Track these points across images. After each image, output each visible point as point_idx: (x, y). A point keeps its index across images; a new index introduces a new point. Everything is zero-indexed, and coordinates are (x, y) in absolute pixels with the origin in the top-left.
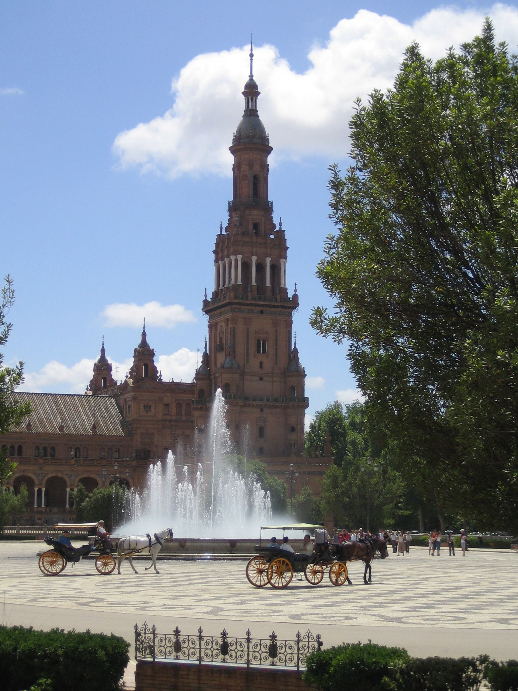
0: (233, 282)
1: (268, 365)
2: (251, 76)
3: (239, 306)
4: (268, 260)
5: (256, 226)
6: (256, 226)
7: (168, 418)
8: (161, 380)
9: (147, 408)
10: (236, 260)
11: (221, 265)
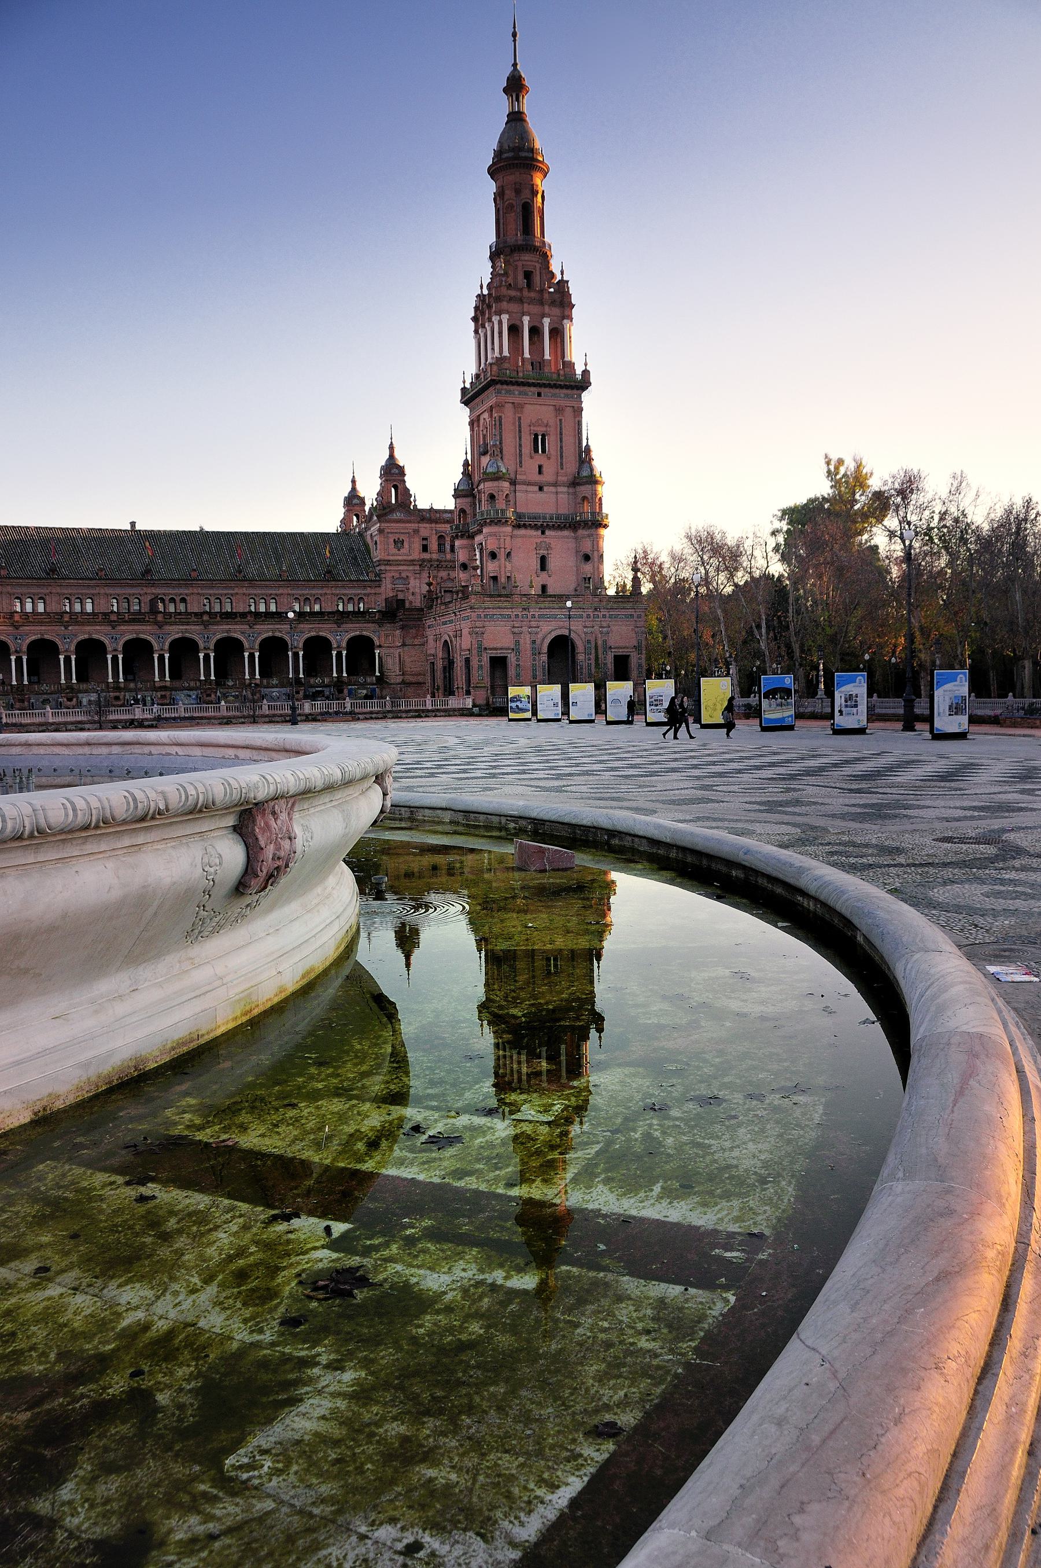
0: (497, 354)
1: (549, 469)
2: (515, 65)
3: (505, 387)
4: (546, 321)
5: (528, 275)
6: (528, 275)
7: (426, 556)
8: (415, 506)
9: (399, 543)
10: (500, 322)
11: (482, 335)
